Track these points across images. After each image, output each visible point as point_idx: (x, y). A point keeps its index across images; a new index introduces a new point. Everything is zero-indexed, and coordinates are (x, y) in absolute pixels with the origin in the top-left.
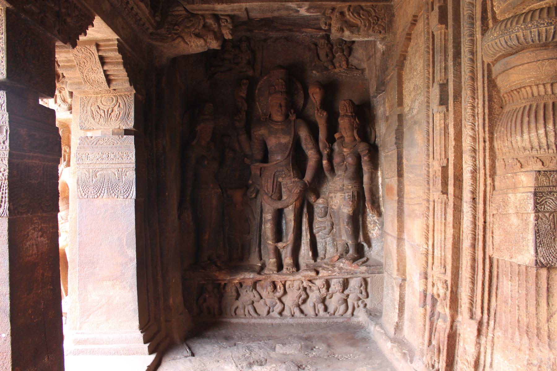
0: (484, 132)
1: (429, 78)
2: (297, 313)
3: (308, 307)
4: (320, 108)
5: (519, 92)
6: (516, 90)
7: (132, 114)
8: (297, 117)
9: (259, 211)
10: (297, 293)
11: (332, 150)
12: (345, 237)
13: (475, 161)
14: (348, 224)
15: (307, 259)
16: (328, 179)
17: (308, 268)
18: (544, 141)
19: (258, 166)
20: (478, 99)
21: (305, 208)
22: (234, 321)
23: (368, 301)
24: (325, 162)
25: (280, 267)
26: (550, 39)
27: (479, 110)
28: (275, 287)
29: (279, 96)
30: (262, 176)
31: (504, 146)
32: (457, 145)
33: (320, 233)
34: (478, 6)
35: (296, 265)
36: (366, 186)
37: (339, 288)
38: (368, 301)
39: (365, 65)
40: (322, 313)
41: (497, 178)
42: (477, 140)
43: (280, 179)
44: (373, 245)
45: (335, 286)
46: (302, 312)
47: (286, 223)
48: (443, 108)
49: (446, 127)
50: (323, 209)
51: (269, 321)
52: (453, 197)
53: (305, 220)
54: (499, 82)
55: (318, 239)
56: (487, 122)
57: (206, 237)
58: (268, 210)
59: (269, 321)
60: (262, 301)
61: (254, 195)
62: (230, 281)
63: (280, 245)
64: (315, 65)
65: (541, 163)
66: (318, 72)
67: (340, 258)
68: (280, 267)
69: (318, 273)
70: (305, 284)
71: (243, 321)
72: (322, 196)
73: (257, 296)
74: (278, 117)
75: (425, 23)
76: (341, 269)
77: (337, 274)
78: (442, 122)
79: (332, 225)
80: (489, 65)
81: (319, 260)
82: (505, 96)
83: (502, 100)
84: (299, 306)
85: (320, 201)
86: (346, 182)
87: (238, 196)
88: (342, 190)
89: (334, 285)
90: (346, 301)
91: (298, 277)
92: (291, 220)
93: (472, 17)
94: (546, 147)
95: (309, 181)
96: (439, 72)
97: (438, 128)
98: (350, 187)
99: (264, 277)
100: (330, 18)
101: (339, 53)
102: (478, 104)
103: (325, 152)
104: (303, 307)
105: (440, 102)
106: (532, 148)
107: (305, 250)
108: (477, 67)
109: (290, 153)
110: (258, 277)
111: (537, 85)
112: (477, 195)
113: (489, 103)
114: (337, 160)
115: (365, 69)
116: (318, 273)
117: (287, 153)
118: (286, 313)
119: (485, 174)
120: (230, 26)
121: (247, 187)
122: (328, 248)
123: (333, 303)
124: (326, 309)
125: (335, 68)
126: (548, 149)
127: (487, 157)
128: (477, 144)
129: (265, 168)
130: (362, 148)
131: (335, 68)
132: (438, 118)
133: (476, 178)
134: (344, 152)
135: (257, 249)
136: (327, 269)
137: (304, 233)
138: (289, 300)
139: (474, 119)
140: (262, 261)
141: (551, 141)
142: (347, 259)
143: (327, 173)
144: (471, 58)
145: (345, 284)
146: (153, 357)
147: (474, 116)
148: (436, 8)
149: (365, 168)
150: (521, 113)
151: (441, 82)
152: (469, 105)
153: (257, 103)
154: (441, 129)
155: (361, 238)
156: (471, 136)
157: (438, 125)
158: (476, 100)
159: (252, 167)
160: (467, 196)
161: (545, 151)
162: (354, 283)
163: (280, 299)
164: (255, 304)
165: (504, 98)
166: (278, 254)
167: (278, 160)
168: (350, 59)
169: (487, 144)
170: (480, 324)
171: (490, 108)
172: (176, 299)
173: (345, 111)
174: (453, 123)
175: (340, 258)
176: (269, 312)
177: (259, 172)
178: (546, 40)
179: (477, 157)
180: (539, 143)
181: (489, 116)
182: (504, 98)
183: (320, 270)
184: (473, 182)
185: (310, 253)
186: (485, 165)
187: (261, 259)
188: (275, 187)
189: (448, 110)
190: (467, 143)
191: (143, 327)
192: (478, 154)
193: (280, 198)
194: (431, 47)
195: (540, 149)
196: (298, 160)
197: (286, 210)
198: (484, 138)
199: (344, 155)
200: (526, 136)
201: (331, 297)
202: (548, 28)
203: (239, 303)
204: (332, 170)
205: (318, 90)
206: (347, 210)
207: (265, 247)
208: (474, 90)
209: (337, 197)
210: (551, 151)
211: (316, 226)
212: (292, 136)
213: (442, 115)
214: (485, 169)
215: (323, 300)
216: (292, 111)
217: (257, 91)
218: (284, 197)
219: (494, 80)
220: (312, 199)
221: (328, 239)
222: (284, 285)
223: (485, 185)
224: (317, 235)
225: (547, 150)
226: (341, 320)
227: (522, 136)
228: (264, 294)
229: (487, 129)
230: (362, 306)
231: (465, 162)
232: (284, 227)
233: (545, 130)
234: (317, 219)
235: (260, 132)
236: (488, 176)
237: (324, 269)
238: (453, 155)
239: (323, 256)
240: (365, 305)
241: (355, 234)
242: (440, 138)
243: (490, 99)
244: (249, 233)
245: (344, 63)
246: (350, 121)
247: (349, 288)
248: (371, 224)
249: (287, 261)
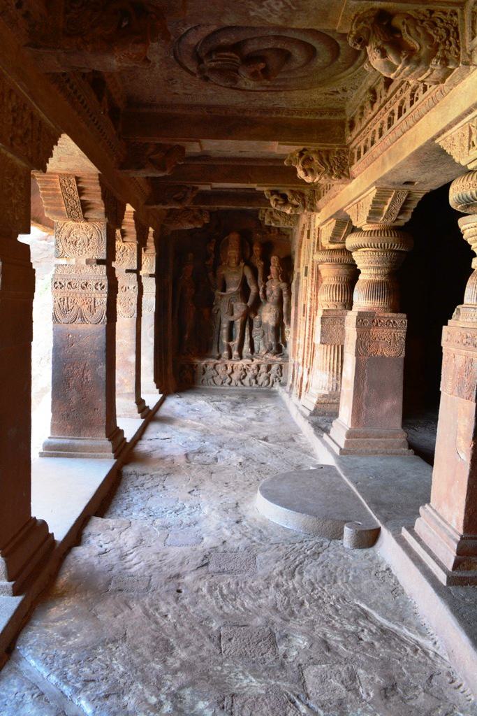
2: (239, 384)
3: (246, 381)
7: (154, 266)
8: (245, 264)
9: (219, 322)
10: (240, 372)
11: (265, 287)
12: (270, 340)
17: (248, 357)
21: (248, 320)
22: (201, 387)
23: (281, 378)
24: (261, 293)
25: (230, 357)
28: (227, 368)
29: (234, 251)
35: (241, 357)
36: (284, 310)
38: (281, 378)
40: (254, 385)
45: (263, 369)
46: (242, 383)
51: (223, 388)
53: (247, 329)
57: (187, 336)
59: (223, 388)
60: (218, 377)
62: (200, 364)
63: (231, 343)
67: (267, 352)
68: (230, 357)
69: (253, 360)
70: (245, 367)
71: (207, 387)
73: (216, 373)
74: (233, 263)
76: (266, 358)
79: (264, 333)
81: (255, 354)
84: (240, 380)
85: (257, 317)
86: (272, 306)
87: (206, 311)
88: (270, 311)
90: (268, 378)
91: (241, 362)
100: (264, 215)
103: (261, 287)
104: (243, 381)
107: (246, 348)
110: (217, 361)
114: (268, 292)
116: (253, 360)
118: (233, 384)
120: (208, 216)
121: (212, 306)
123: (261, 379)
124: (257, 382)
125: (270, 232)
130: (283, 285)
134: (273, 286)
136: (259, 359)
137: (246, 337)
138: (235, 376)
143: (262, 300)
145: (269, 368)
146: (161, 395)
149: (285, 299)
155: (280, 341)
159: (215, 294)
162: (274, 367)
163: (229, 375)
164: (214, 378)
166: (230, 349)
170: (309, 369)
172: (170, 370)
175: (267, 352)
176: (222, 383)
177: (220, 298)
183: (254, 359)
187: (219, 351)
191: (155, 380)
193: (232, 314)
196: (244, 291)
197: (235, 322)
201: (260, 376)
203: (205, 377)
204: (265, 297)
205: (258, 249)
206: (272, 323)
208: (313, 274)
209: (267, 316)
211: (254, 333)
212: (241, 276)
215: (255, 377)
220: (252, 316)
222: (232, 367)
226: (265, 389)
228: (220, 371)
230: (278, 381)
232: (234, 333)
234: (255, 328)
240: (280, 381)
241: (277, 338)
243: (318, 279)
249: (235, 353)
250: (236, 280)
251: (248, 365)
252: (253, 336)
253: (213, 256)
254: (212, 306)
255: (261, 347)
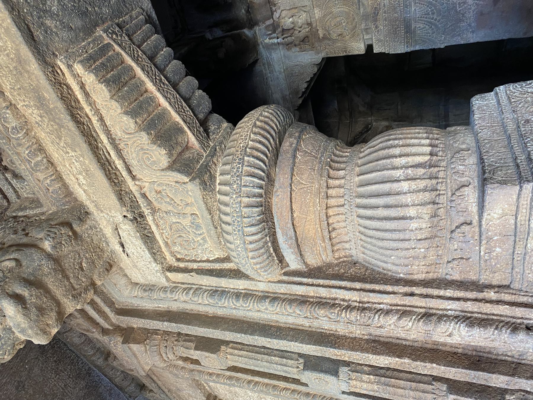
0: (394, 293)
1: (294, 391)
5: (334, 229)
6: (330, 232)
13: (446, 316)
18: (422, 184)
20: (335, 299)
26: (264, 167)
27: (354, 299)
31: (425, 257)
32: (411, 354)
34: (201, 282)
41: (484, 279)
42: (408, 309)
48: (343, 370)
49: (376, 371)
52: (516, 379)
54: (313, 261)
56: (377, 287)
65: (466, 189)
75: (216, 380)
78: (365, 377)
80: (285, 274)
82: (337, 255)
83: (344, 262)
93: (215, 292)
94: (434, 181)
96: (285, 368)
97: (376, 387)
102: (344, 300)
105: (333, 375)
106: (434, 203)
108: (286, 294)
111: (327, 197)
112: (519, 321)
113: (344, 280)
119: (476, 300)
126: (437, 178)
127: (442, 293)
128: (415, 310)
132: (358, 384)
133: (484, 320)
139: (369, 309)
141: (424, 174)
144: (270, 301)
147: (364, 309)
148: (196, 354)
150: (368, 223)
151: (301, 367)
152: (343, 315)
154: (378, 383)
156: (399, 318)
157: (370, 386)
158: (337, 302)
160: (521, 341)
161: (442, 183)
165: (340, 258)
169: (417, 290)
171: (353, 279)
174: (371, 356)
178: (264, 172)
179: (441, 312)
180: (425, 190)
181: (367, 282)
182: (340, 258)
184: (491, 325)
186: (458, 299)
189: (347, 364)
190: (412, 331)
192: (434, 311)
194: (250, 377)
195: (437, 190)
198: (406, 294)
200: (412, 212)
202: (246, 163)
210: (441, 174)
213: (354, 375)
214: (466, 300)
219: (311, 270)
223: (498, 302)
225: (440, 180)
227: (411, 218)
229: (389, 288)
231: (450, 335)
233: (404, 180)
236: (480, 295)
238: (429, 365)
242: (393, 386)
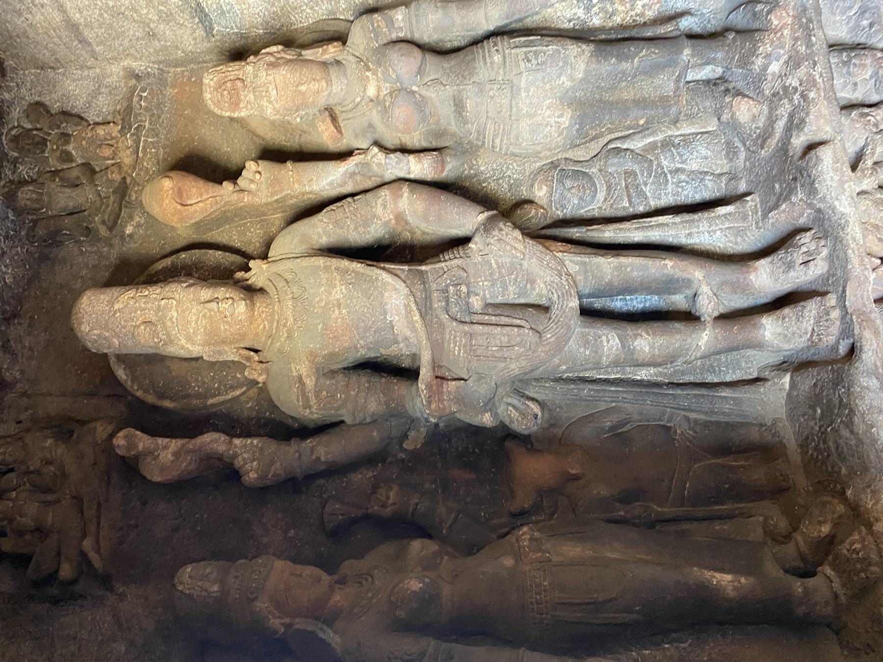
4: (235, 183)
9: (586, 390)
14: (628, 58)
15: (745, 218)
16: (471, 177)
19: (429, 387)
30: (466, 378)
33: (647, 190)
37: (868, 61)
39: (115, 72)
43: (476, 303)
44: (680, 6)
47: (627, 290)
50: (568, 183)
53: (609, 234)
55: (666, 200)
58: (586, 343)
61: (535, 408)
64: (103, 222)
66: (131, 218)
72: (525, 194)
76: (794, 62)
77: (819, 68)
81: (743, 187)
85: (540, 193)
87: (534, 469)
89: (855, 84)
92: (619, 268)
95: (479, 208)
98: (497, 58)
99: (867, 334)
101: (70, 148)
109: (384, 269)
115: (125, 69)
117: (384, 275)
122: (694, 166)
129: (435, 365)
131: (119, 165)
135: (726, 393)
140: (766, 374)
142: (753, 52)
143: (450, 169)
153: (210, 401)
167: (407, 306)
168: (92, 117)
173: (239, 84)
183: (799, 141)
185: (722, 210)
188: (504, 320)
199: (391, 94)
205: (167, 183)
207: (711, 369)
211: (624, 206)
216: (240, 275)
217: (167, 404)
218: (537, 293)
221: (665, 163)
224: (654, 204)
235: (310, 383)
237: (795, 124)
239: (724, 179)
244: (667, 429)
245: (101, 131)
246: (272, 65)
247: (862, 40)
248: (613, 14)
250: (339, 292)
251: (854, 168)
252: (641, 209)
253: (213, 441)
254: (504, 436)
255: (694, 165)
